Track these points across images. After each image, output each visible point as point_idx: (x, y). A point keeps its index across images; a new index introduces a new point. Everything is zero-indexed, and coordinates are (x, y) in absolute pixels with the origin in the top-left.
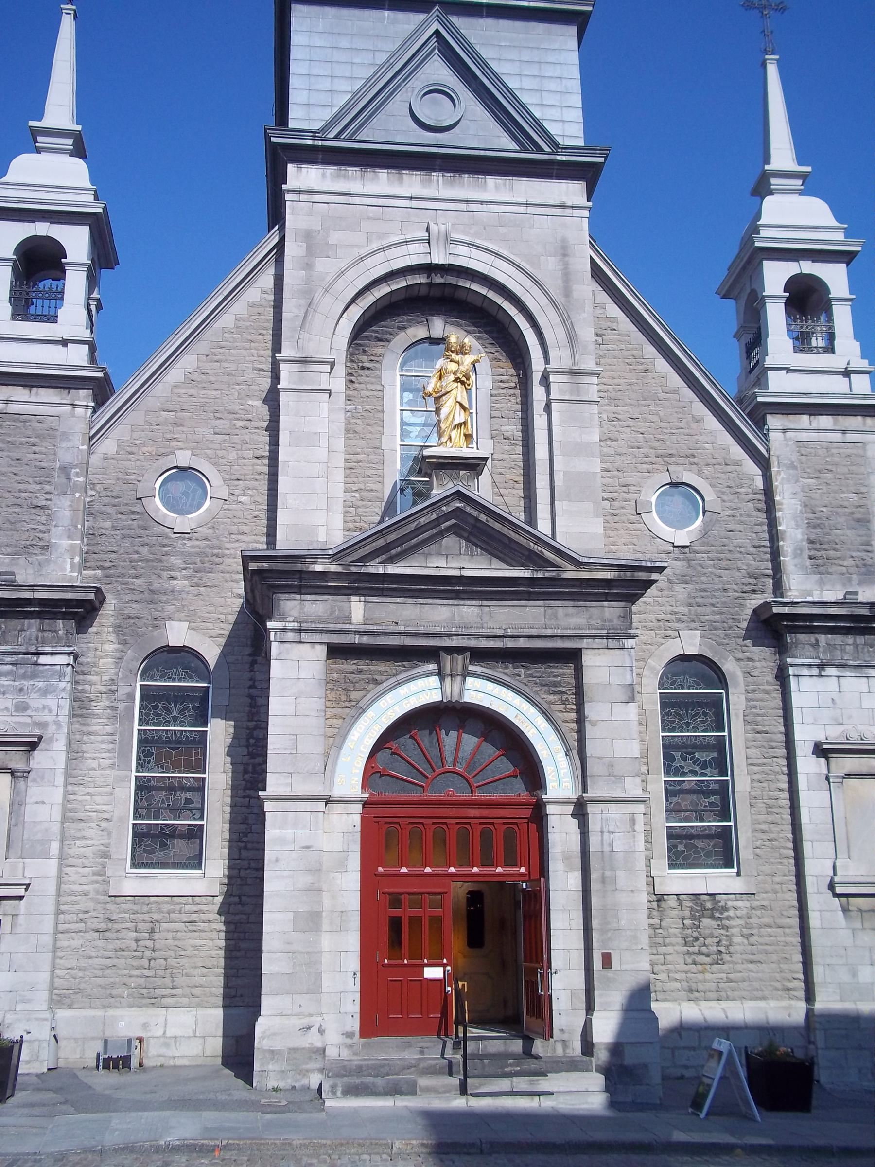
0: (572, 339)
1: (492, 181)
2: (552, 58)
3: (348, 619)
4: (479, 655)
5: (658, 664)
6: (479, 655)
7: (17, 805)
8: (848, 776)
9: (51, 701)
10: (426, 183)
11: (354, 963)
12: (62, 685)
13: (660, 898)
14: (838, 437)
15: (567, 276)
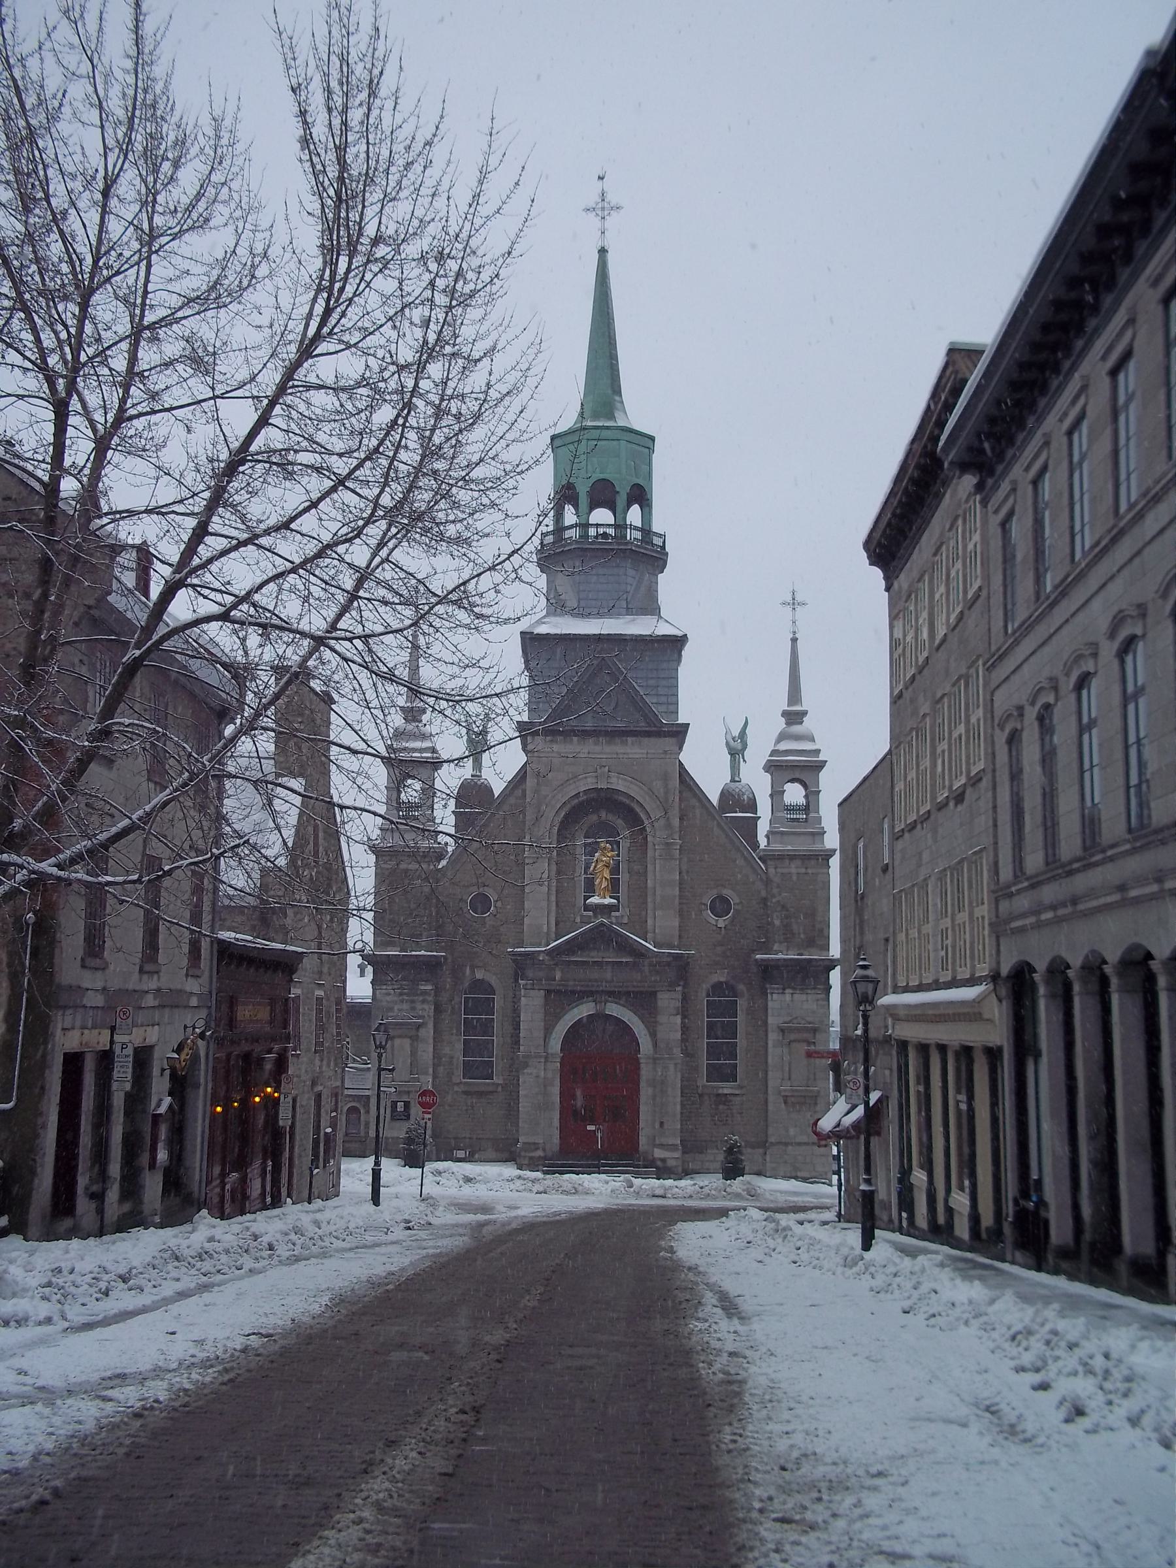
0: (669, 826)
1: (630, 739)
2: (665, 665)
3: (554, 980)
4: (611, 994)
5: (705, 986)
6: (611, 994)
7: (414, 1053)
8: (795, 1041)
9: (426, 1006)
10: (596, 744)
11: (556, 1123)
12: (430, 998)
13: (701, 1096)
14: (803, 870)
15: (666, 793)
